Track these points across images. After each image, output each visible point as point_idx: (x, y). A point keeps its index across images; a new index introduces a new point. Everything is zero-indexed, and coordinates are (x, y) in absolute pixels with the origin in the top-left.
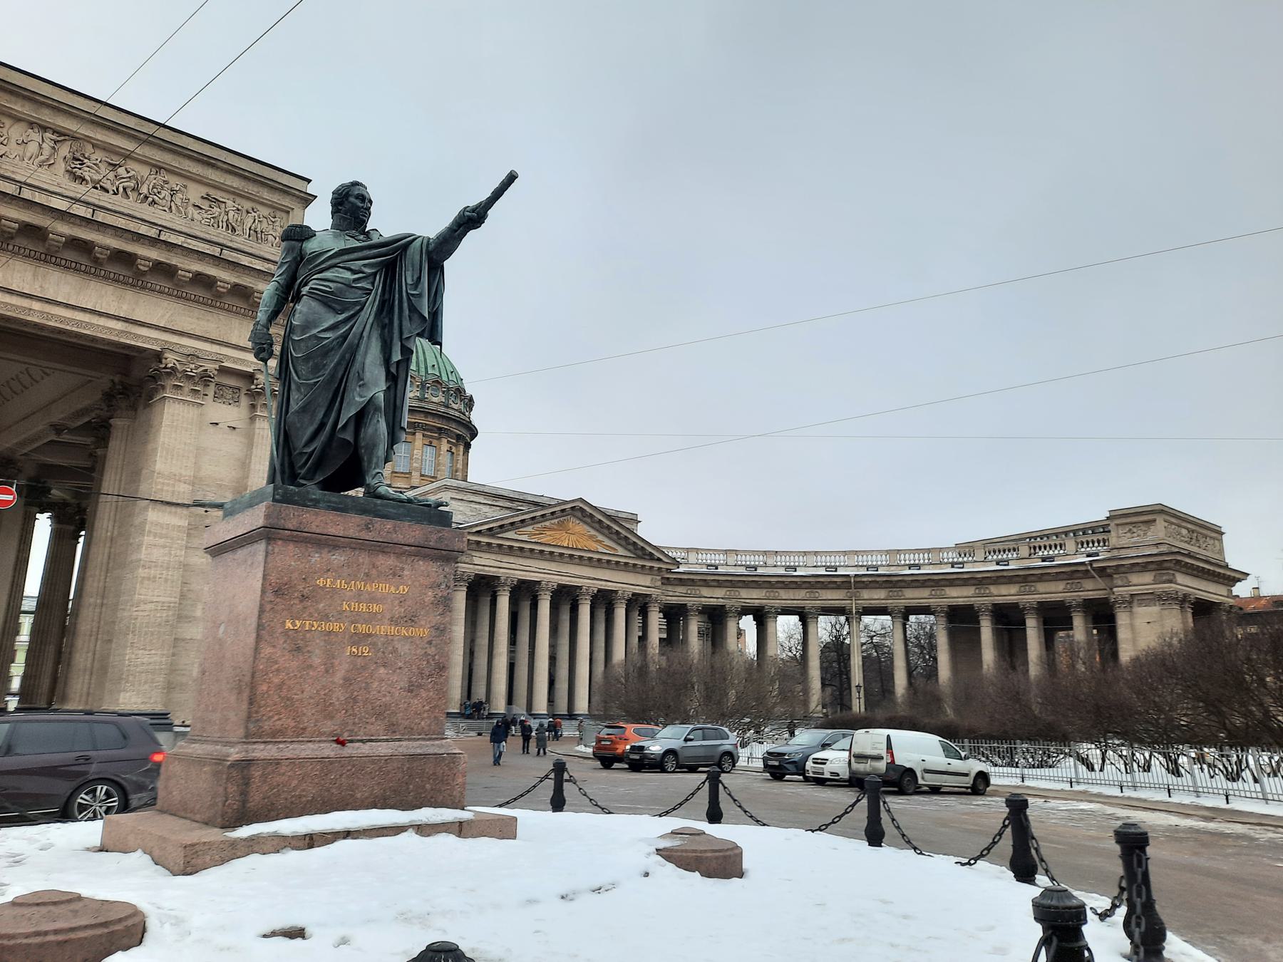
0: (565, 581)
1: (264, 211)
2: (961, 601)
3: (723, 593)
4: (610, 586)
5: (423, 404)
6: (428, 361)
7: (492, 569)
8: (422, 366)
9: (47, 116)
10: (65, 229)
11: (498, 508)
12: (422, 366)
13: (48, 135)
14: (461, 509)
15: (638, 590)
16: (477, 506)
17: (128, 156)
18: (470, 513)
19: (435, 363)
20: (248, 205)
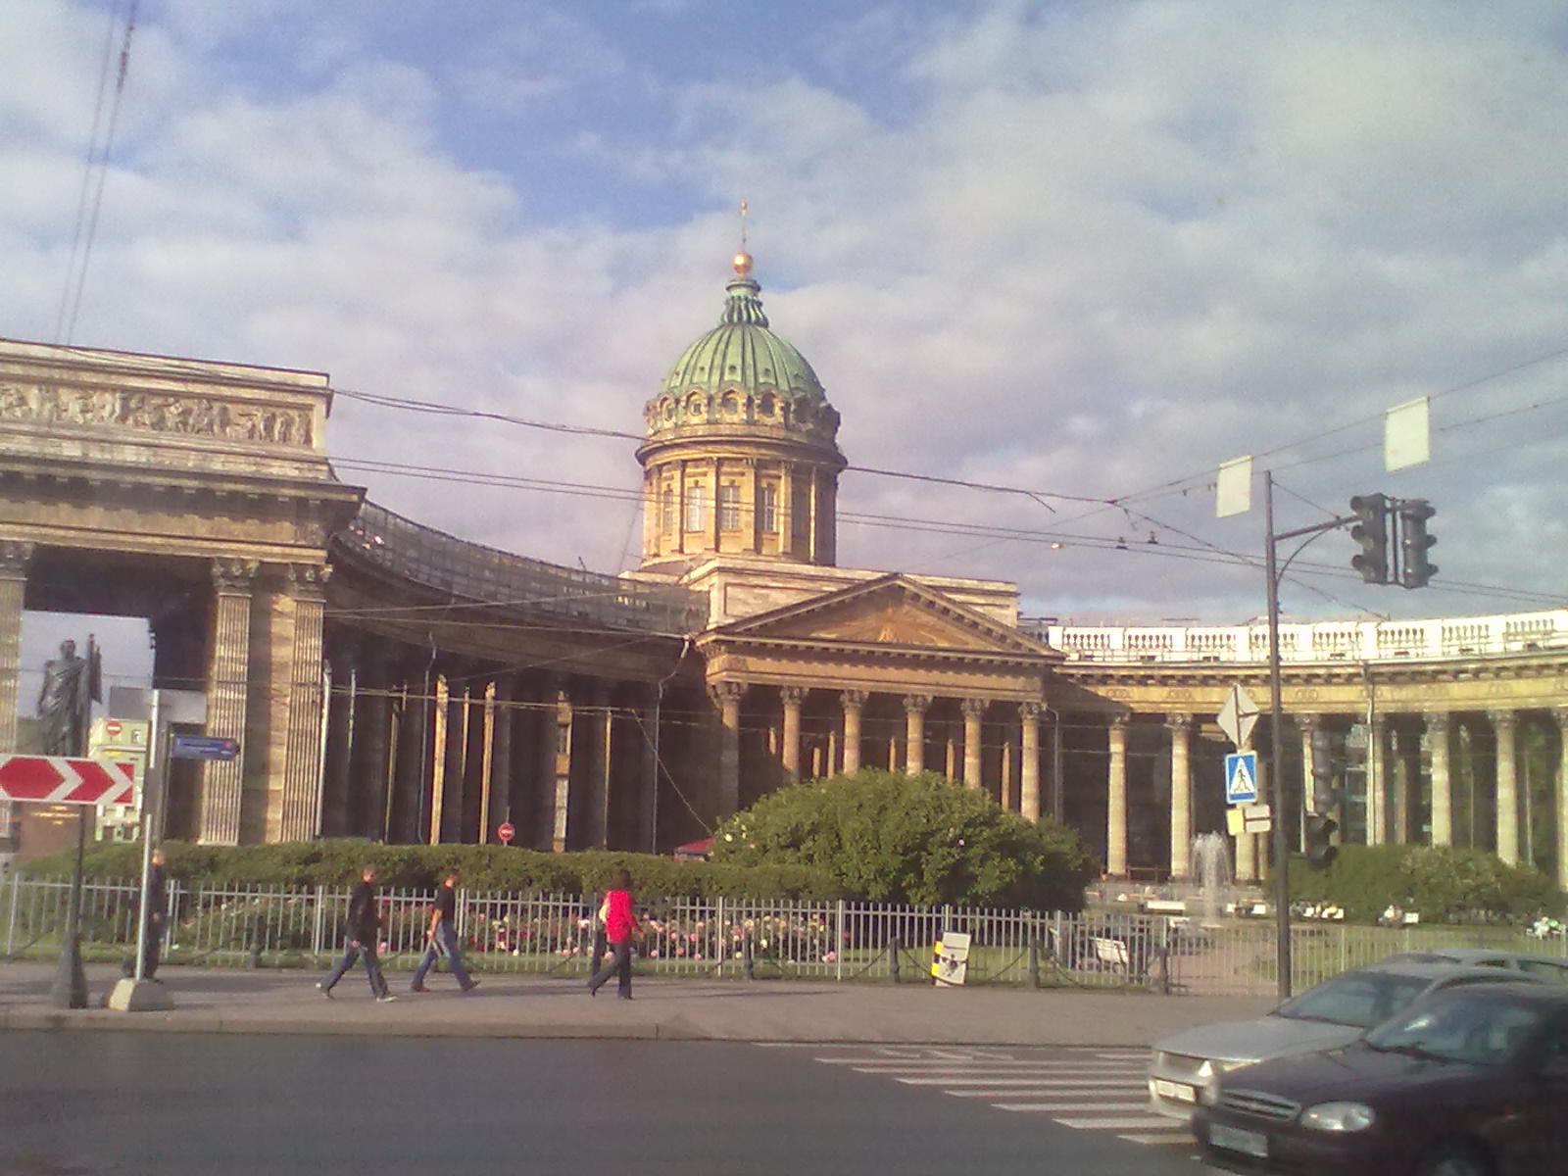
0: (883, 688)
1: (294, 413)
2: (1533, 703)
3: (1165, 694)
4: (954, 693)
5: (754, 430)
6: (759, 365)
7: (771, 677)
8: (750, 372)
9: (114, 380)
10: (129, 478)
11: (793, 592)
12: (750, 372)
13: (117, 395)
14: (741, 596)
15: (1000, 696)
16: (764, 591)
17: (176, 395)
18: (754, 601)
19: (770, 367)
20: (278, 412)
